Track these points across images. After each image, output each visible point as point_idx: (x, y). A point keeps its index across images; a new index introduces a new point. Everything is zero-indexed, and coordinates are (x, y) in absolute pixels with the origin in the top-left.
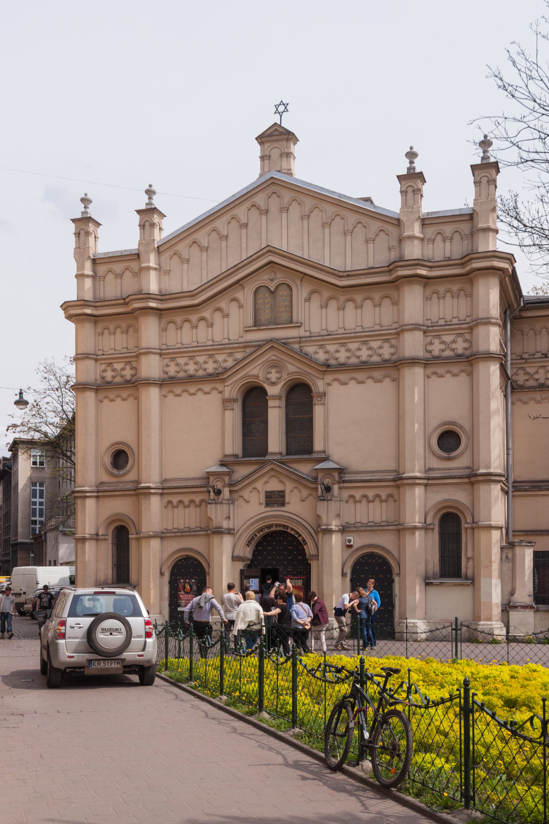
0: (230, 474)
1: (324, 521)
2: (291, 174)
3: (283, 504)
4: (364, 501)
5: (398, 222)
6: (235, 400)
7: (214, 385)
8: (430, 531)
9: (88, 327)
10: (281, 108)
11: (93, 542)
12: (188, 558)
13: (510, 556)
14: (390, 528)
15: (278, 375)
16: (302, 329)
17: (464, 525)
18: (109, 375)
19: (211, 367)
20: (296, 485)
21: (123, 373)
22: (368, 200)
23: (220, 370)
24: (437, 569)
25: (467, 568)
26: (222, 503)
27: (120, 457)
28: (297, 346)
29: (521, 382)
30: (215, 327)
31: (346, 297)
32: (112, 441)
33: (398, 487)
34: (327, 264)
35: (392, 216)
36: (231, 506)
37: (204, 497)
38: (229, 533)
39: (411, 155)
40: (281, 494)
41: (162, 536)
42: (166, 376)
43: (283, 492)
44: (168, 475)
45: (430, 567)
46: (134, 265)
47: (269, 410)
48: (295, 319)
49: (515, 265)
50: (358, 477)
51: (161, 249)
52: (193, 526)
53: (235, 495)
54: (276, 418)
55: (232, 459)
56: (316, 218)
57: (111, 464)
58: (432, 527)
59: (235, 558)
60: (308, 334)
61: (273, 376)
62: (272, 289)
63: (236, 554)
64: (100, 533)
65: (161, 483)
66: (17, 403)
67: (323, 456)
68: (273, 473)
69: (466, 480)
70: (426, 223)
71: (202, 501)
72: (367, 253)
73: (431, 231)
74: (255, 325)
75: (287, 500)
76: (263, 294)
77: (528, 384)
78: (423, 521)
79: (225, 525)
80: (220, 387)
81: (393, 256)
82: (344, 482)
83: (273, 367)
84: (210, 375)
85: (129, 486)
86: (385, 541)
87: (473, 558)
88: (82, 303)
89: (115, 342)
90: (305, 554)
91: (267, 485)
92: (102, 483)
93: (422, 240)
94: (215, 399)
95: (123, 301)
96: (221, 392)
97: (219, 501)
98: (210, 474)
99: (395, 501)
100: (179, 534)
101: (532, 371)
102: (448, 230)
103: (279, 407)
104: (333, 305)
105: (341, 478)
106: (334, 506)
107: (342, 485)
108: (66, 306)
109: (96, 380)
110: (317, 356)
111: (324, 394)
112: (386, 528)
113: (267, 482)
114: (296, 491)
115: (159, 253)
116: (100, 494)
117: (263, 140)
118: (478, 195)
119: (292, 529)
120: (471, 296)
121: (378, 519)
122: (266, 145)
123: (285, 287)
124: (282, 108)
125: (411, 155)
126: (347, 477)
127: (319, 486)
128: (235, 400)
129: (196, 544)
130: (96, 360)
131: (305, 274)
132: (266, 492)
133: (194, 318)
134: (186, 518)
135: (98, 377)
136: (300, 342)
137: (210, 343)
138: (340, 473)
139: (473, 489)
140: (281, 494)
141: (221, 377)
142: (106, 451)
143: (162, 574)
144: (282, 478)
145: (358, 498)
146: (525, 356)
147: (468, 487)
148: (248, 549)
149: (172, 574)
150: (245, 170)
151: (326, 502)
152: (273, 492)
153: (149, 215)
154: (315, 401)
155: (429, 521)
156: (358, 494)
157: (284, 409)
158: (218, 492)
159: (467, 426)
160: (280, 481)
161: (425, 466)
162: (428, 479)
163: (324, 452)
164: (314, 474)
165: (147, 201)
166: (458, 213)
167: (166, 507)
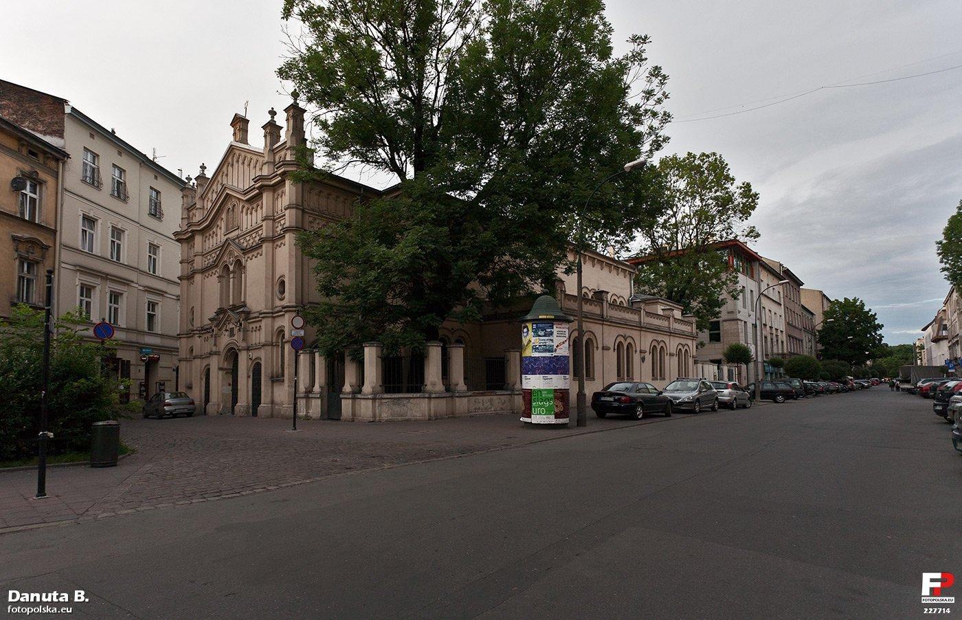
63: (221, 366)
76: (231, 213)
79: (214, 349)
109: (188, 274)
111: (245, 267)
136: (238, 238)
143: (201, 379)
158: (213, 331)
161: (272, 305)
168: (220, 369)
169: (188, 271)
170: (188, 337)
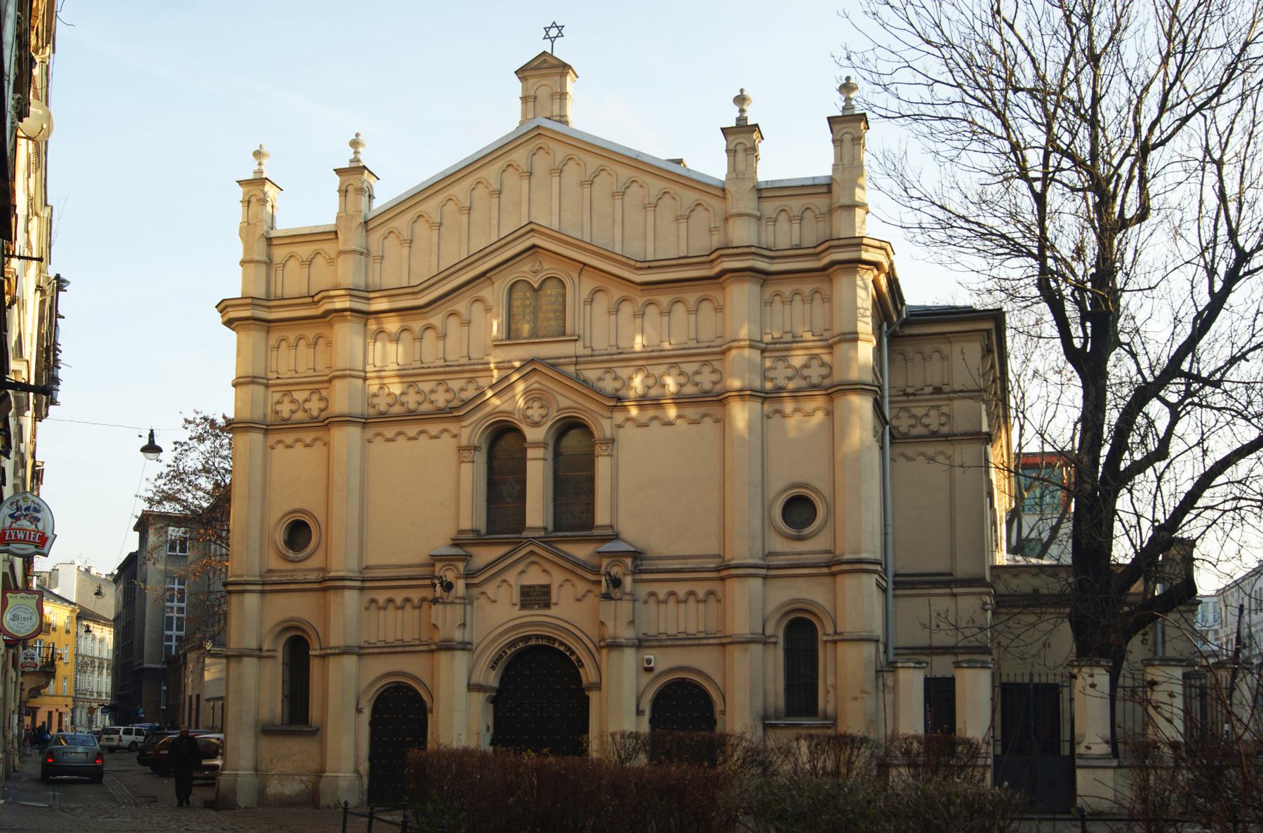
0: (466, 558)
1: (610, 630)
2: (566, 123)
3: (547, 605)
4: (672, 600)
5: (721, 191)
6: (476, 448)
7: (446, 426)
8: (772, 646)
9: (255, 336)
10: (554, 32)
11: (254, 660)
12: (399, 687)
13: (890, 682)
14: (711, 641)
15: (543, 412)
16: (580, 344)
17: (821, 637)
18: (285, 409)
19: (441, 399)
20: (567, 576)
21: (307, 406)
22: (679, 162)
23: (455, 403)
24: (781, 703)
25: (827, 702)
26: (453, 603)
27: (298, 532)
28: (571, 369)
29: (903, 429)
30: (448, 340)
31: (645, 299)
32: (287, 508)
33: (723, 579)
34: (618, 249)
35: (715, 183)
36: (468, 607)
37: (428, 593)
38: (464, 649)
39: (741, 100)
40: (545, 590)
41: (360, 652)
42: (372, 411)
43: (548, 586)
44: (372, 561)
45: (771, 700)
46: (330, 248)
47: (529, 464)
48: (569, 329)
49: (892, 257)
50: (663, 565)
51: (371, 225)
52: (408, 637)
53: (475, 592)
54: (537, 474)
55: (470, 536)
56: (603, 185)
57: (285, 542)
58: (773, 640)
59: (472, 687)
60: (588, 351)
61: (536, 413)
62: (536, 286)
63: (475, 680)
64: (265, 648)
65: (360, 572)
66: (144, 450)
67: (610, 532)
68: (532, 558)
69: (825, 570)
70: (765, 194)
71: (423, 600)
72: (678, 236)
73: (770, 207)
74: (509, 338)
75: (554, 599)
77: (914, 432)
78: (760, 631)
79: (458, 635)
80: (453, 427)
81: (716, 241)
82: (641, 572)
83: (535, 399)
84: (440, 410)
85: (313, 576)
86: (701, 661)
87: (835, 687)
88: (249, 300)
89: (294, 360)
90: (581, 681)
91: (524, 576)
92: (269, 571)
93: (759, 219)
94: (447, 444)
95: (310, 300)
96: (455, 436)
97: (450, 599)
98: (436, 558)
99: (719, 601)
100: (387, 650)
101: (919, 412)
102: (795, 205)
103: (544, 459)
104: (627, 309)
105: (636, 567)
106: (625, 607)
107: (638, 577)
108: (223, 307)
109: (265, 416)
110: (601, 384)
112: (705, 642)
113: (523, 572)
114: (568, 585)
115: (367, 231)
116: (267, 588)
117: (526, 74)
118: (839, 157)
119: (562, 643)
120: (828, 300)
121: (692, 629)
122: (531, 81)
123: (555, 282)
124: (554, 31)
125: (741, 100)
126: (646, 565)
127: (603, 579)
128: (476, 448)
129: (412, 666)
130: (267, 386)
131: (585, 264)
132: (522, 587)
133: (417, 325)
134: (397, 625)
135: (269, 411)
136: (576, 364)
137: (442, 363)
138: (635, 559)
139: (835, 584)
140: (545, 590)
141: (455, 414)
142: (278, 523)
143: (359, 711)
144: (547, 566)
145: (662, 596)
146: (910, 390)
147: (828, 580)
148: (493, 673)
149: (375, 710)
150: (500, 114)
151: (613, 602)
152: (533, 587)
153: (353, 176)
154: (598, 450)
155: (769, 631)
156: (662, 590)
157: (550, 462)
158: (448, 587)
159: (826, 491)
160: (544, 571)
162: (769, 568)
163: (611, 527)
164: (595, 561)
165: (352, 157)
166: (811, 183)
167: (367, 609)
168: (472, 687)
169: (264, 403)
170: (262, 592)
